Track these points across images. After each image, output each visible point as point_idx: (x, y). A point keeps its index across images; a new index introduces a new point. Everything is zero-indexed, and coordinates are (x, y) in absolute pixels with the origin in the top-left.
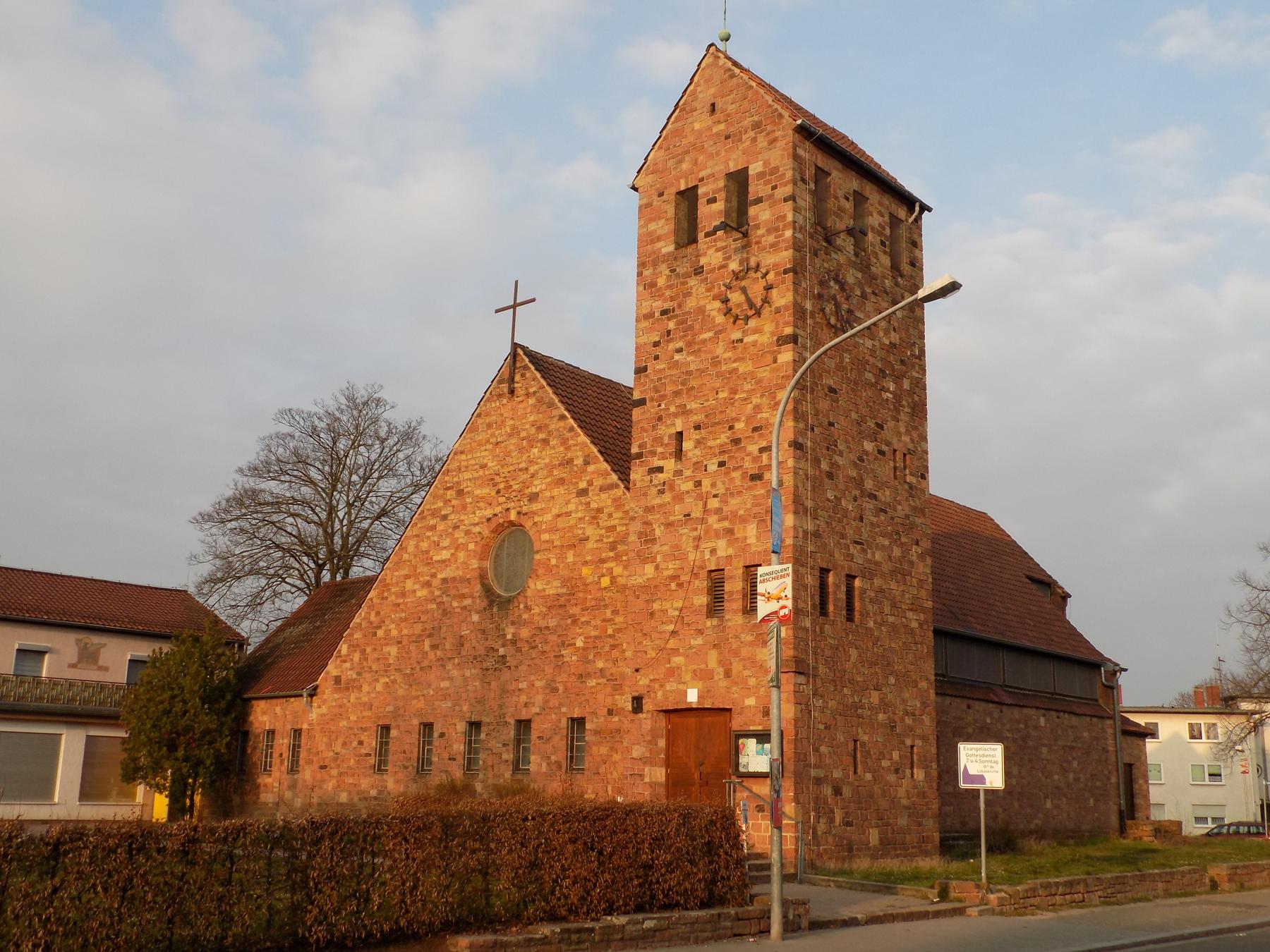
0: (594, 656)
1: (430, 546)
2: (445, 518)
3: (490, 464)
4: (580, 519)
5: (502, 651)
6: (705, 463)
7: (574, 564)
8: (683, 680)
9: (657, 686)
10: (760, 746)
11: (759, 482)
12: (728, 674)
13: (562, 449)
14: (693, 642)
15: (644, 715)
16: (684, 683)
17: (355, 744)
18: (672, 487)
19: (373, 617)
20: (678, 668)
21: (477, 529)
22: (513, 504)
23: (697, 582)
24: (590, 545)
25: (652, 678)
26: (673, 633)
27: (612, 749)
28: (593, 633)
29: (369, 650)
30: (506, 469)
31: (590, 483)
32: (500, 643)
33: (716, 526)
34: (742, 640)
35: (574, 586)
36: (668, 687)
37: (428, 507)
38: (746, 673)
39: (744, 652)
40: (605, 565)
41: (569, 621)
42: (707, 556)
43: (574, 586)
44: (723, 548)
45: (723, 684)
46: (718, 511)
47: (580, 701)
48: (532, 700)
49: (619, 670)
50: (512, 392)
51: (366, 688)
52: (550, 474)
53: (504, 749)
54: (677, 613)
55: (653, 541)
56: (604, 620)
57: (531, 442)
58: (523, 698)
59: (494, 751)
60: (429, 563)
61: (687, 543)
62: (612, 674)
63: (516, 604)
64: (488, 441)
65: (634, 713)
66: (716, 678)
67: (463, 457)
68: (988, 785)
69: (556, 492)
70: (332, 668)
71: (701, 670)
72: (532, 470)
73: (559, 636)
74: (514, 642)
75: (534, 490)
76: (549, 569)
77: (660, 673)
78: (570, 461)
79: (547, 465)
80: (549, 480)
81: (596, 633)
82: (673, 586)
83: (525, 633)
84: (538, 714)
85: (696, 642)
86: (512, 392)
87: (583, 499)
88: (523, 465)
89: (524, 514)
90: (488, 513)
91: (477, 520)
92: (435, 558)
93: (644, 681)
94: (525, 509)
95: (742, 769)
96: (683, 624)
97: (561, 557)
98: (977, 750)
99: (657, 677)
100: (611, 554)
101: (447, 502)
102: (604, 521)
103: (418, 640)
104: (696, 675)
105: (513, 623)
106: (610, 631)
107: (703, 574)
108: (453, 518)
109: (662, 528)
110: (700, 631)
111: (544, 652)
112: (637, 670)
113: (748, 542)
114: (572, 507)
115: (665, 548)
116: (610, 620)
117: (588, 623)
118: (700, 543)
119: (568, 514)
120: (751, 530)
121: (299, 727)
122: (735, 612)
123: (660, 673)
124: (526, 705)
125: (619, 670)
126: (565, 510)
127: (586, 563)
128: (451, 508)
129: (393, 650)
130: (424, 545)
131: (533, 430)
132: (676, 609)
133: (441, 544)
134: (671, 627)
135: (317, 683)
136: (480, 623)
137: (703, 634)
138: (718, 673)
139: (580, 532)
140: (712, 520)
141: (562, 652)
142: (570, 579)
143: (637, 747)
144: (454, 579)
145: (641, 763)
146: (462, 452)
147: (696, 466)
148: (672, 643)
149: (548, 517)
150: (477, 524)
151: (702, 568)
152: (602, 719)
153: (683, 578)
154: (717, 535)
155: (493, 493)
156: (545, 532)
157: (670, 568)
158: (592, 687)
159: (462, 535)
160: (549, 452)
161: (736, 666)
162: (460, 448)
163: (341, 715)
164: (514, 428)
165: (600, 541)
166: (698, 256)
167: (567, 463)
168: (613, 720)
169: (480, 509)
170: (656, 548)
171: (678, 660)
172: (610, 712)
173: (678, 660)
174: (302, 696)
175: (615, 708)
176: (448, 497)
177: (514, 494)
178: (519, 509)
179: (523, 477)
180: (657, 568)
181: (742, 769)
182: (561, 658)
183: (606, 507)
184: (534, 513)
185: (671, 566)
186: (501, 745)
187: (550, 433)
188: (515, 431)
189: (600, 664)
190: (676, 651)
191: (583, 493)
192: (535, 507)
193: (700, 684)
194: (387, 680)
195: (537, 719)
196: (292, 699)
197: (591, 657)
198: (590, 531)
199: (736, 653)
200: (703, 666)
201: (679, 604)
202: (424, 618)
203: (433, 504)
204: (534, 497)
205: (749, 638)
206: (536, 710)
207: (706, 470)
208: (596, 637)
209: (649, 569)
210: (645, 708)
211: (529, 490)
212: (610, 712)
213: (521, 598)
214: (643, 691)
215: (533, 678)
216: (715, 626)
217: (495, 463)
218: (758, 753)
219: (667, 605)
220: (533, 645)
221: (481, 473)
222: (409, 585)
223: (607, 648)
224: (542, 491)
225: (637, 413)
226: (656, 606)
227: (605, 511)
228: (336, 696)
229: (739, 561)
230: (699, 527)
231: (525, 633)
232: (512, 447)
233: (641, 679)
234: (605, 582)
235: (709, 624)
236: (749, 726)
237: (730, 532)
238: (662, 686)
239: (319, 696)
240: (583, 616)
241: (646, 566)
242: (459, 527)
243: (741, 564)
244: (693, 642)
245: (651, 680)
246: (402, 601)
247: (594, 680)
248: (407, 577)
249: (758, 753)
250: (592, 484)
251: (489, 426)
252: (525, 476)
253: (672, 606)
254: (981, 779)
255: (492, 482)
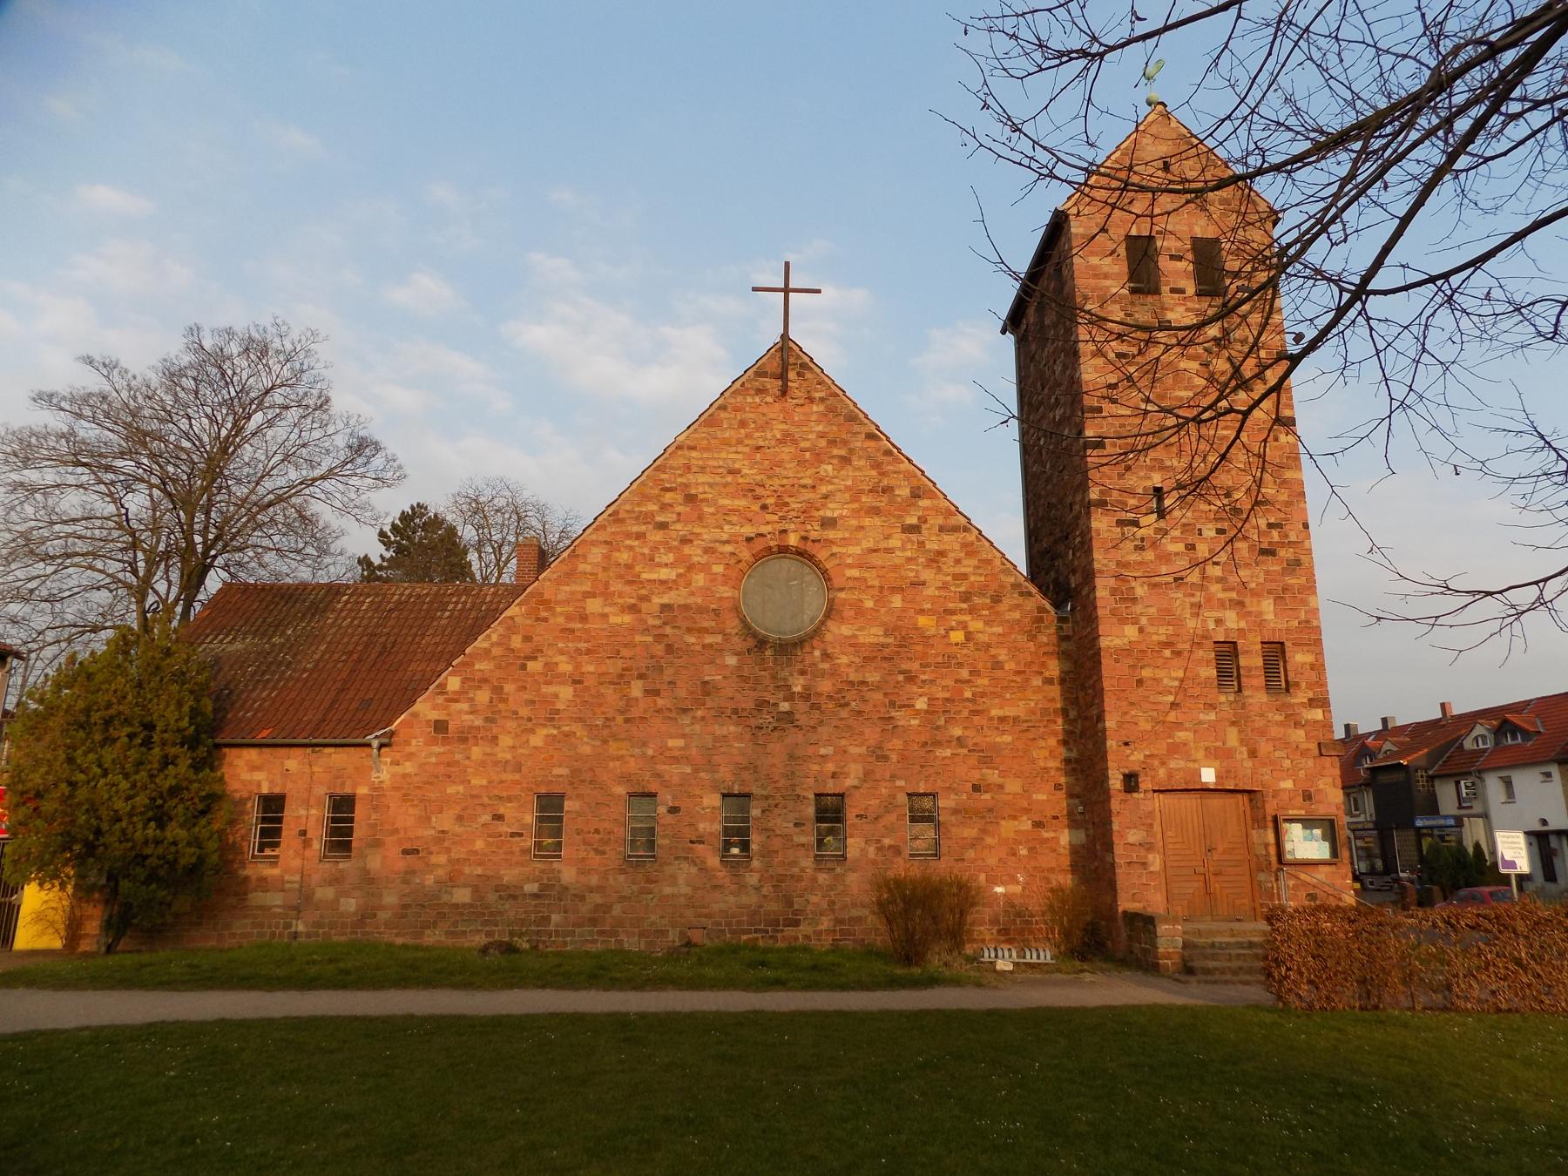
0: (946, 722)
1: (634, 559)
2: (663, 526)
3: (745, 471)
4: (909, 560)
5: (785, 706)
6: (1198, 527)
7: (904, 610)
8: (1193, 758)
9: (1156, 763)
10: (1308, 831)
11: (1270, 558)
12: (1253, 754)
13: (874, 473)
14: (1202, 716)
15: (1142, 795)
16: (1195, 761)
17: (486, 818)
18: (1154, 544)
19: (516, 642)
20: (1185, 745)
21: (728, 548)
22: (793, 526)
23: (1201, 653)
24: (930, 591)
25: (1147, 753)
26: (1174, 705)
27: (984, 831)
28: (941, 695)
29: (509, 688)
30: (777, 482)
31: (923, 520)
32: (781, 695)
33: (1221, 595)
34: (1270, 719)
35: (904, 639)
36: (1173, 764)
37: (628, 507)
38: (1277, 754)
39: (1274, 731)
40: (954, 617)
41: (901, 678)
42: (1212, 625)
43: (904, 639)
44: (1232, 620)
45: (1249, 764)
46: (1220, 580)
47: (927, 774)
48: (846, 770)
49: (987, 739)
50: (784, 392)
51: (506, 741)
52: (855, 499)
53: (797, 830)
54: (1176, 683)
55: (1134, 600)
56: (957, 681)
57: (819, 458)
58: (830, 767)
59: (778, 832)
60: (635, 581)
61: (1183, 609)
62: (976, 744)
63: (807, 649)
64: (740, 442)
65: (1125, 791)
66: (1238, 757)
67: (694, 454)
68: (1518, 871)
69: (867, 521)
70: (425, 708)
71: (1216, 748)
72: (824, 489)
73: (885, 694)
74: (805, 696)
75: (829, 514)
76: (860, 612)
77: (1161, 748)
78: (887, 490)
79: (848, 489)
80: (856, 505)
81: (947, 695)
82: (1167, 653)
83: (825, 686)
84: (856, 787)
85: (1208, 718)
86: (784, 392)
87: (914, 537)
88: (808, 482)
89: (813, 541)
90: (748, 530)
91: (725, 537)
92: (644, 576)
93: (1137, 757)
94: (814, 535)
95: (1289, 857)
96: (1185, 695)
97: (880, 601)
98: (1508, 837)
99: (1156, 752)
100: (964, 606)
101: (664, 507)
102: (948, 565)
103: (621, 680)
104: (1211, 753)
105: (803, 673)
106: (968, 694)
107: (1209, 644)
108: (680, 529)
109: (1146, 587)
110: (1211, 705)
111: (860, 713)
112: (1126, 744)
113: (1265, 617)
114: (895, 542)
115: (1153, 610)
116: (968, 681)
117: (932, 682)
118: (1201, 611)
119: (889, 551)
120: (1267, 607)
121: (348, 790)
122: (1257, 688)
123: (1161, 748)
124: (834, 775)
125: (987, 739)
126: (883, 545)
127: (922, 612)
128: (675, 516)
129: (566, 692)
130: (624, 557)
131: (823, 443)
132: (1176, 679)
133: (657, 560)
134: (1171, 698)
135: (392, 727)
136: (739, 668)
137: (1215, 709)
138: (1241, 753)
139: (913, 574)
140: (1215, 588)
141: (893, 714)
142: (897, 628)
143: (1132, 831)
144: (686, 607)
145: (1142, 850)
146: (693, 448)
147: (1187, 528)
148: (1172, 717)
149: (857, 550)
150: (727, 542)
151: (1205, 637)
152: (964, 796)
153: (1180, 647)
154: (1222, 604)
155: (756, 507)
156: (850, 566)
157: (1162, 633)
158: (944, 758)
159: (699, 552)
160: (848, 472)
161: (1264, 747)
162: (688, 442)
163: (449, 777)
164: (786, 434)
165: (945, 586)
166: (1163, 309)
167: (884, 491)
168: (982, 797)
169: (729, 523)
170: (1138, 609)
171: (1182, 735)
172: (976, 788)
173: (1182, 735)
174: (369, 745)
175: (982, 783)
176: (667, 501)
177: (794, 514)
178: (803, 534)
179: (808, 495)
180: (1141, 630)
181: (1289, 857)
182: (892, 721)
183: (953, 551)
184: (832, 542)
185: (1162, 630)
186: (791, 825)
187: (851, 451)
188: (787, 439)
189: (957, 732)
190: (1178, 726)
191: (914, 529)
192: (831, 534)
193: (1217, 763)
194: (555, 732)
195: (857, 794)
196: (327, 750)
197: (941, 722)
198: (927, 575)
199: (1263, 732)
200: (1219, 744)
201: (1180, 674)
202: (625, 652)
203: (638, 505)
204: (828, 523)
205: (1279, 718)
206: (849, 782)
207: (1201, 534)
208: (947, 700)
209: (1131, 632)
210: (1143, 786)
211: (821, 513)
212: (976, 788)
213: (815, 643)
214: (1137, 768)
215: (843, 742)
216: (1231, 703)
217: (755, 470)
218: (1305, 839)
219: (1161, 673)
220: (842, 701)
221: (729, 479)
222: (594, 606)
223: (965, 713)
224: (842, 517)
225: (1093, 457)
226: (1146, 673)
227: (951, 555)
228: (437, 749)
229: (1256, 636)
230: (1198, 594)
231: (825, 686)
232: (787, 458)
233: (1132, 753)
234: (957, 636)
235: (1223, 698)
236: (1287, 809)
237: (1241, 604)
238: (1163, 763)
239: (395, 748)
240: (924, 673)
241: (1126, 627)
242: (691, 541)
243: (1259, 639)
244: (1202, 716)
245: (1146, 756)
246: (580, 626)
247: (949, 750)
248: (592, 595)
249: (1305, 839)
250: (925, 522)
251: (743, 424)
252: (811, 496)
253: (1171, 676)
254: (1512, 864)
255: (750, 491)
